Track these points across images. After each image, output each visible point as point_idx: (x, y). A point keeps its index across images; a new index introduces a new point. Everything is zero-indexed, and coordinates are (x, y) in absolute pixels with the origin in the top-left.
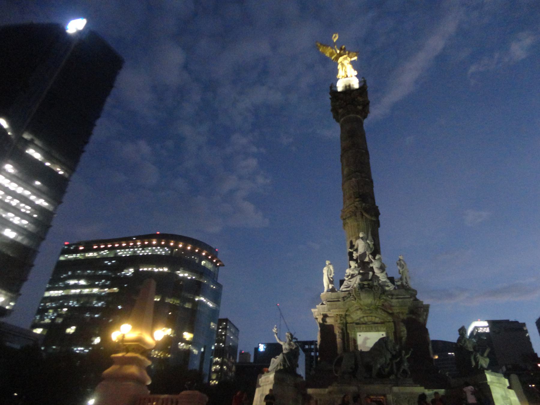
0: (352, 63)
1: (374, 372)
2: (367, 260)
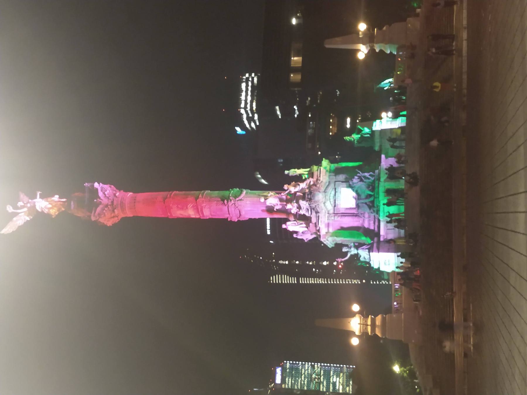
2: (284, 197)
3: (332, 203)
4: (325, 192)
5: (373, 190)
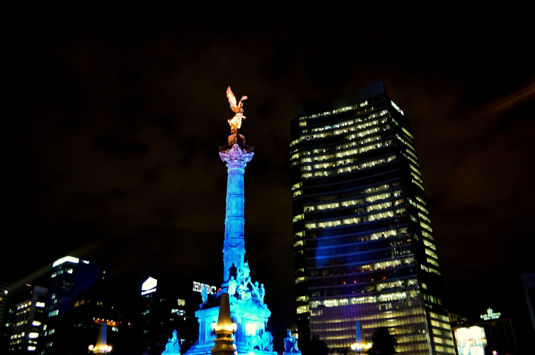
0: (243, 118)
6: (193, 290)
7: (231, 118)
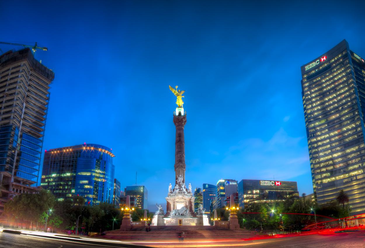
0: (183, 99)
1: (180, 214)
3: (178, 201)
4: (182, 198)
5: (182, 215)
6: (261, 185)
7: (176, 101)
